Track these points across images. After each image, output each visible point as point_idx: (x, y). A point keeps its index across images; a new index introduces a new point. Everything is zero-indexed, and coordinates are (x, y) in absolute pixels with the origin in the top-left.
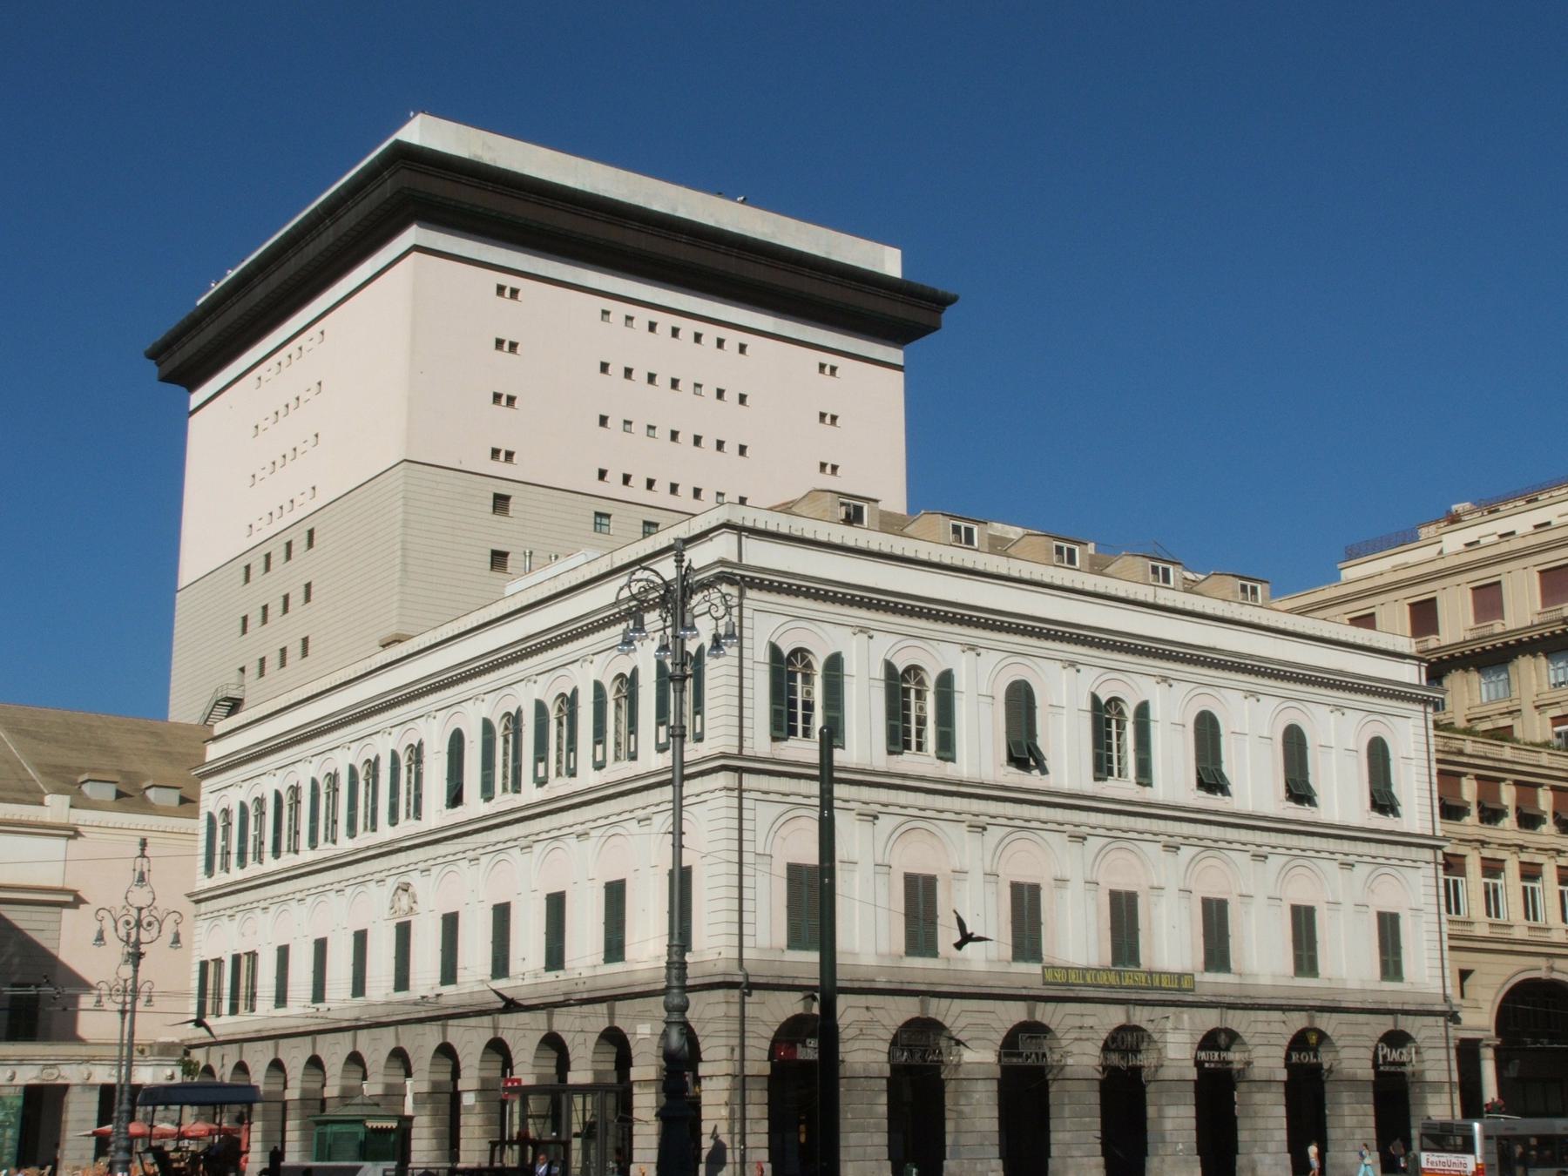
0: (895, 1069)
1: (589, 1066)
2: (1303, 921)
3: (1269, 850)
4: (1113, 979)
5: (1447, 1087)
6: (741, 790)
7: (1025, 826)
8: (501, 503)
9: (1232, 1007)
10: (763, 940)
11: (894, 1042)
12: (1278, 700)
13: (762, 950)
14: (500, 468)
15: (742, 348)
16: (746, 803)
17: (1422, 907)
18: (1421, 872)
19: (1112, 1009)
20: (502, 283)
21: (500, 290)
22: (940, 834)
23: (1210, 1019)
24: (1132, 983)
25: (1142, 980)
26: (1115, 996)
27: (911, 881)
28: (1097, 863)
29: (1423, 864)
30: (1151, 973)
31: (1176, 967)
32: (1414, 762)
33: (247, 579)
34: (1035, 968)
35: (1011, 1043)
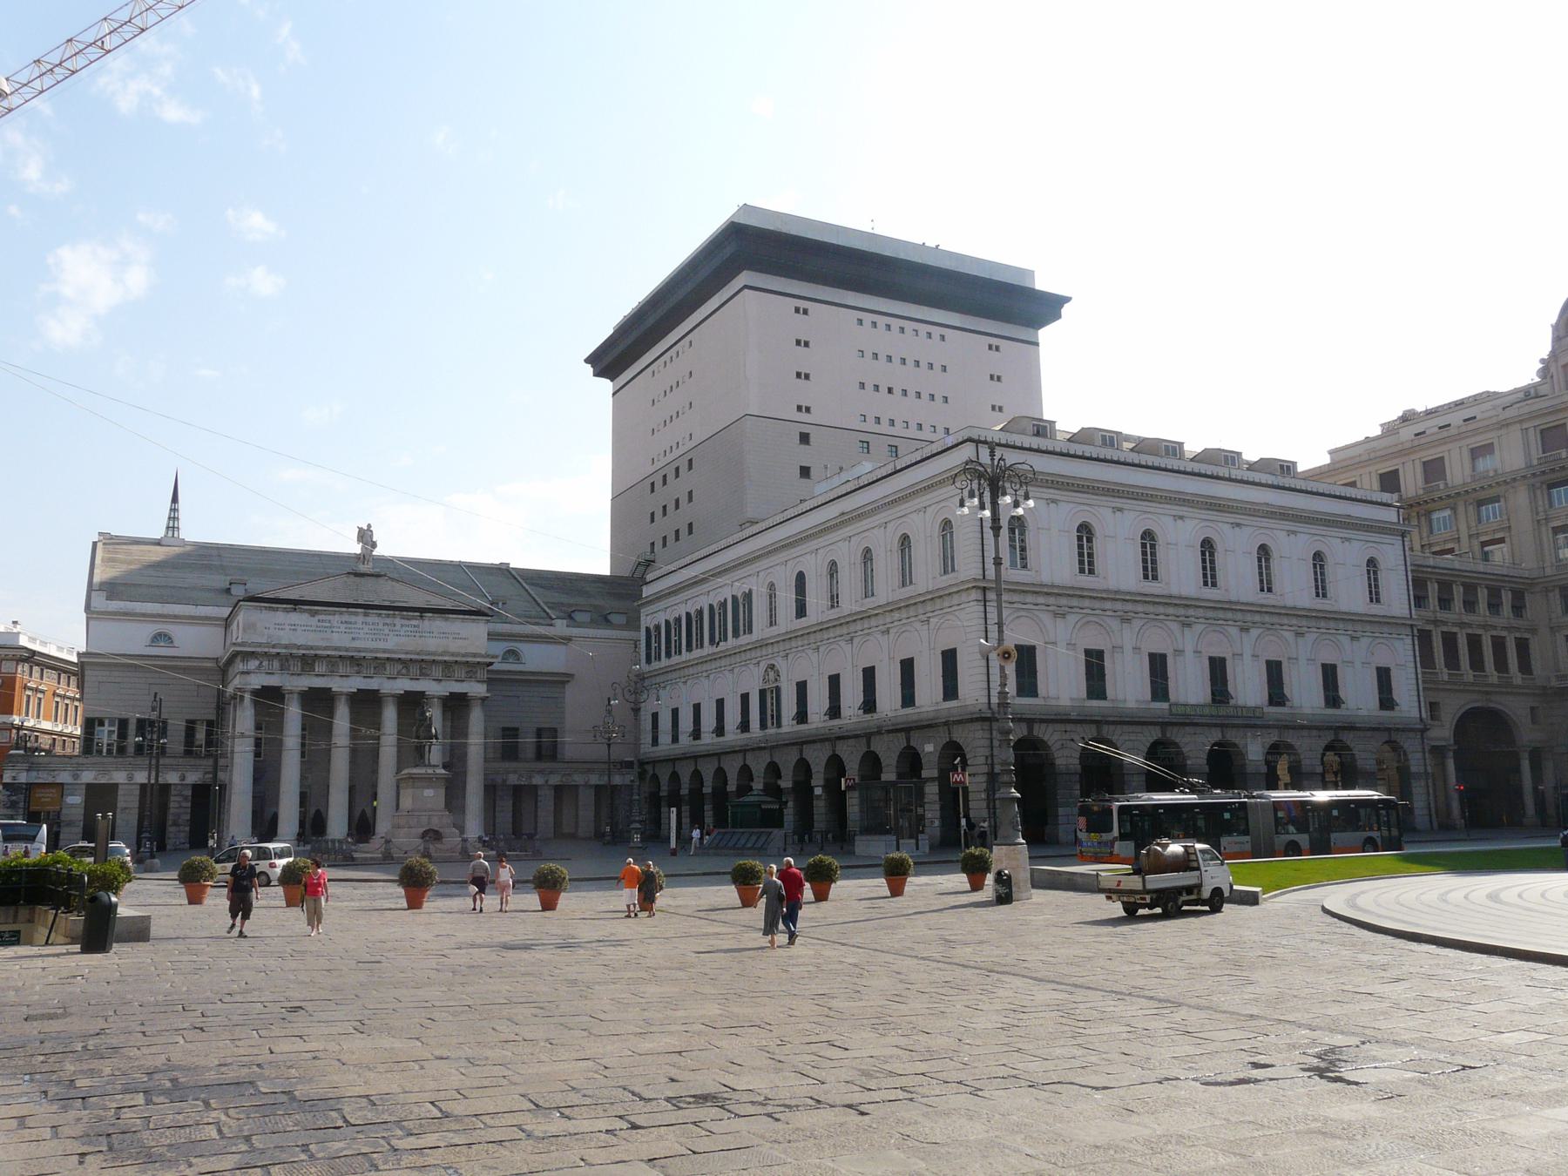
0: (1084, 767)
1: (895, 770)
2: (1330, 674)
6: (985, 601)
8: (804, 438)
9: (1287, 727)
12: (1308, 536)
14: (803, 417)
15: (943, 338)
20: (798, 305)
21: (797, 310)
23: (1274, 737)
25: (1231, 711)
30: (1236, 707)
31: (1251, 703)
33: (653, 491)
34: (1165, 705)
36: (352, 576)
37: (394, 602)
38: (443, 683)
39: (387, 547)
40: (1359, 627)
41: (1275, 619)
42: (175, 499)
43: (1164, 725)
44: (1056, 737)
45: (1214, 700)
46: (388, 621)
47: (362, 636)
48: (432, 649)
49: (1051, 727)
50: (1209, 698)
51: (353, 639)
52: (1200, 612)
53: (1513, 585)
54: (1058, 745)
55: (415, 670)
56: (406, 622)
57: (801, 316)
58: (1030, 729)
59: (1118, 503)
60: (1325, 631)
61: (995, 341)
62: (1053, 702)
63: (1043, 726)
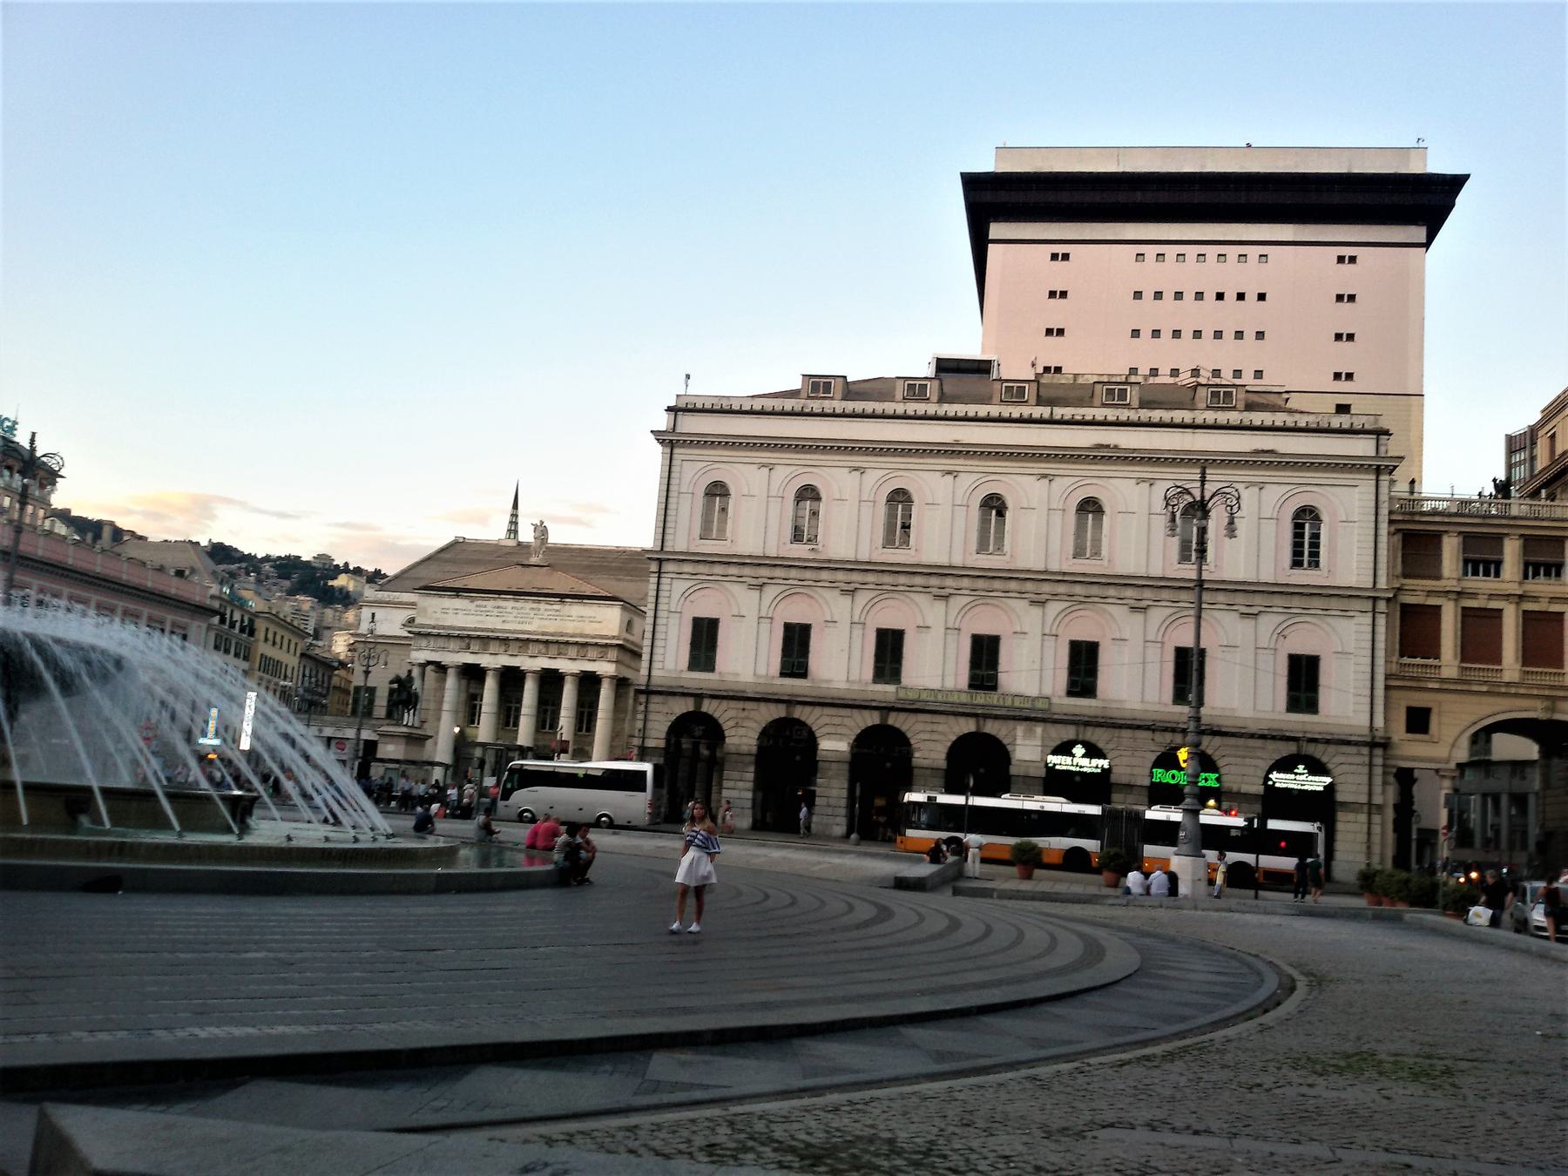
0: (759, 747)
4: (964, 698)
5: (1365, 808)
6: (660, 572)
7: (894, 589)
9: (1087, 724)
13: (670, 671)
16: (663, 581)
18: (1355, 620)
19: (962, 720)
22: (816, 596)
26: (965, 711)
27: (788, 628)
28: (964, 612)
29: (1359, 614)
32: (1356, 524)
34: (891, 688)
35: (865, 740)
36: (520, 567)
37: (539, 589)
38: (577, 662)
39: (556, 537)
40: (1258, 600)
41: (1095, 590)
43: (886, 709)
44: (731, 713)
45: (971, 686)
46: (535, 606)
48: (570, 631)
49: (725, 703)
50: (963, 681)
51: (504, 621)
52: (965, 582)
54: (731, 723)
55: (553, 649)
58: (698, 704)
59: (858, 460)
62: (731, 678)
63: (715, 703)
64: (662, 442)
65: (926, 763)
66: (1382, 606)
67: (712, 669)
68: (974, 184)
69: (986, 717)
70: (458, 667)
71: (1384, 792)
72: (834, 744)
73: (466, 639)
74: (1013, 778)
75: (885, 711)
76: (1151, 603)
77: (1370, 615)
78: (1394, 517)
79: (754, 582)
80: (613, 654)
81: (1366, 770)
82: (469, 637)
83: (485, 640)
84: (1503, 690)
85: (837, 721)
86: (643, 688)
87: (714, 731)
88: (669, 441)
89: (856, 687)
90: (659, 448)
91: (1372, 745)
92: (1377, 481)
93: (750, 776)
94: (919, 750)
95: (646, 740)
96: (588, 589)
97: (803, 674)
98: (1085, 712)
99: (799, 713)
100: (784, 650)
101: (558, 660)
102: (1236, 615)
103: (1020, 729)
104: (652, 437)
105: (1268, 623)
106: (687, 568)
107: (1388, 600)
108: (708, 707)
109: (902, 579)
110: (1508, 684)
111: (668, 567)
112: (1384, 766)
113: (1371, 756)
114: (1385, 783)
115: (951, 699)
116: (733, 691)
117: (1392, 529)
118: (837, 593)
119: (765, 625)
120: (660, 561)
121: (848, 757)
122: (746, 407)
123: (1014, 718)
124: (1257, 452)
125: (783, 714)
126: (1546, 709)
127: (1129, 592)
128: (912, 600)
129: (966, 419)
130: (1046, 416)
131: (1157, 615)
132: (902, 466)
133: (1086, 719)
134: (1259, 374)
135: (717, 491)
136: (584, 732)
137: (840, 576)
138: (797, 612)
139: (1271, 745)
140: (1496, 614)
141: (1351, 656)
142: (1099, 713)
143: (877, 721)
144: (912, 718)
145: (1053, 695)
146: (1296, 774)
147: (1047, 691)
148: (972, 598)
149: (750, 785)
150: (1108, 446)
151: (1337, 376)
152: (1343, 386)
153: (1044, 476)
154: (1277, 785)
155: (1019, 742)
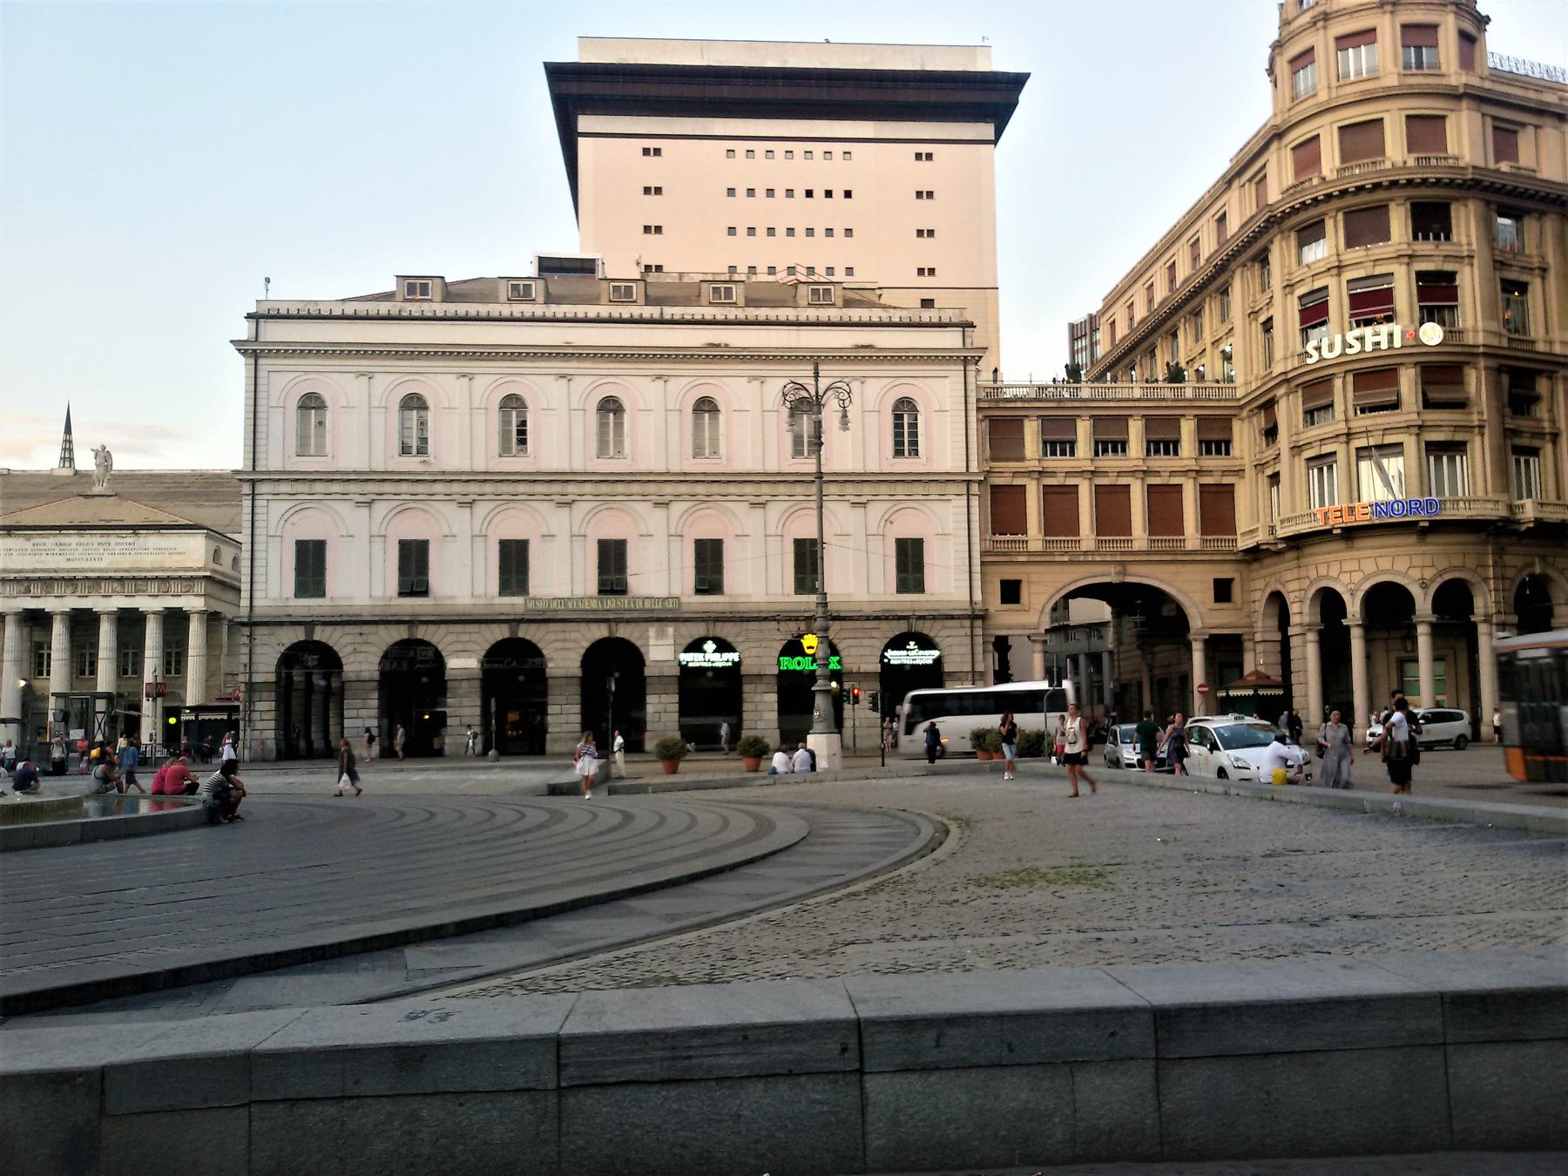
0: (382, 673)
3: (769, 498)
4: (594, 605)
5: (970, 676)
6: (253, 494)
9: (716, 620)
10: (274, 592)
11: (386, 656)
13: (275, 599)
16: (258, 503)
17: (951, 532)
19: (594, 627)
22: (431, 511)
24: (613, 606)
27: (405, 546)
28: (588, 518)
32: (948, 413)
34: (518, 600)
35: (496, 653)
36: (82, 498)
37: (107, 521)
38: (159, 598)
39: (121, 463)
40: (866, 489)
41: (716, 488)
42: (68, 430)
43: (515, 622)
45: (601, 592)
46: (103, 540)
47: (76, 556)
49: (339, 630)
50: (592, 587)
52: (588, 488)
53: (1145, 412)
54: (350, 649)
55: (130, 586)
56: (122, 540)
57: (652, 159)
58: (310, 632)
60: (803, 498)
61: (924, 148)
63: (329, 629)
64: (244, 353)
65: (560, 672)
66: (975, 488)
67: (323, 595)
68: (558, 74)
69: (618, 621)
70: (16, 614)
71: (985, 659)
72: (463, 662)
73: (25, 582)
74: (648, 680)
75: (514, 624)
76: (769, 498)
77: (966, 497)
78: (982, 405)
79: (362, 499)
80: (200, 588)
81: (968, 640)
82: (27, 579)
83: (48, 582)
84: (1082, 558)
85: (465, 638)
86: (246, 620)
87: (330, 660)
88: (252, 351)
89: (482, 602)
90: (241, 359)
91: (973, 617)
92: (965, 370)
93: (375, 703)
94: (552, 659)
95: (254, 675)
96: (165, 519)
97: (424, 593)
98: (714, 608)
99: (422, 633)
100: (401, 569)
101: (137, 598)
102: (847, 505)
103: (652, 630)
104: (232, 347)
105: (877, 510)
106: (285, 488)
107: (980, 482)
108: (320, 634)
109: (521, 488)
110: (1086, 553)
111: (261, 488)
112: (984, 635)
113: (972, 628)
114: (985, 652)
115: (582, 607)
116: (347, 615)
117: (980, 417)
118: (454, 505)
119: (378, 545)
120: (253, 482)
121: (479, 674)
122: (337, 312)
123: (646, 620)
124: (858, 347)
125: (405, 636)
126: (1118, 573)
127: (748, 489)
128: (533, 508)
129: (575, 320)
130: (656, 316)
131: (775, 510)
132: (515, 371)
133: (715, 615)
134: (849, 271)
135: (312, 403)
136: (173, 675)
137: (456, 488)
138: (412, 529)
139: (884, 625)
140: (1228, 489)
141: (951, 537)
142: (728, 608)
143: (506, 634)
144: (544, 628)
145: (682, 594)
146: (908, 650)
147: (676, 591)
148: (595, 504)
149: (375, 712)
150: (718, 346)
151: (921, 271)
152: (926, 281)
153: (659, 377)
154: (892, 662)
155: (652, 642)
